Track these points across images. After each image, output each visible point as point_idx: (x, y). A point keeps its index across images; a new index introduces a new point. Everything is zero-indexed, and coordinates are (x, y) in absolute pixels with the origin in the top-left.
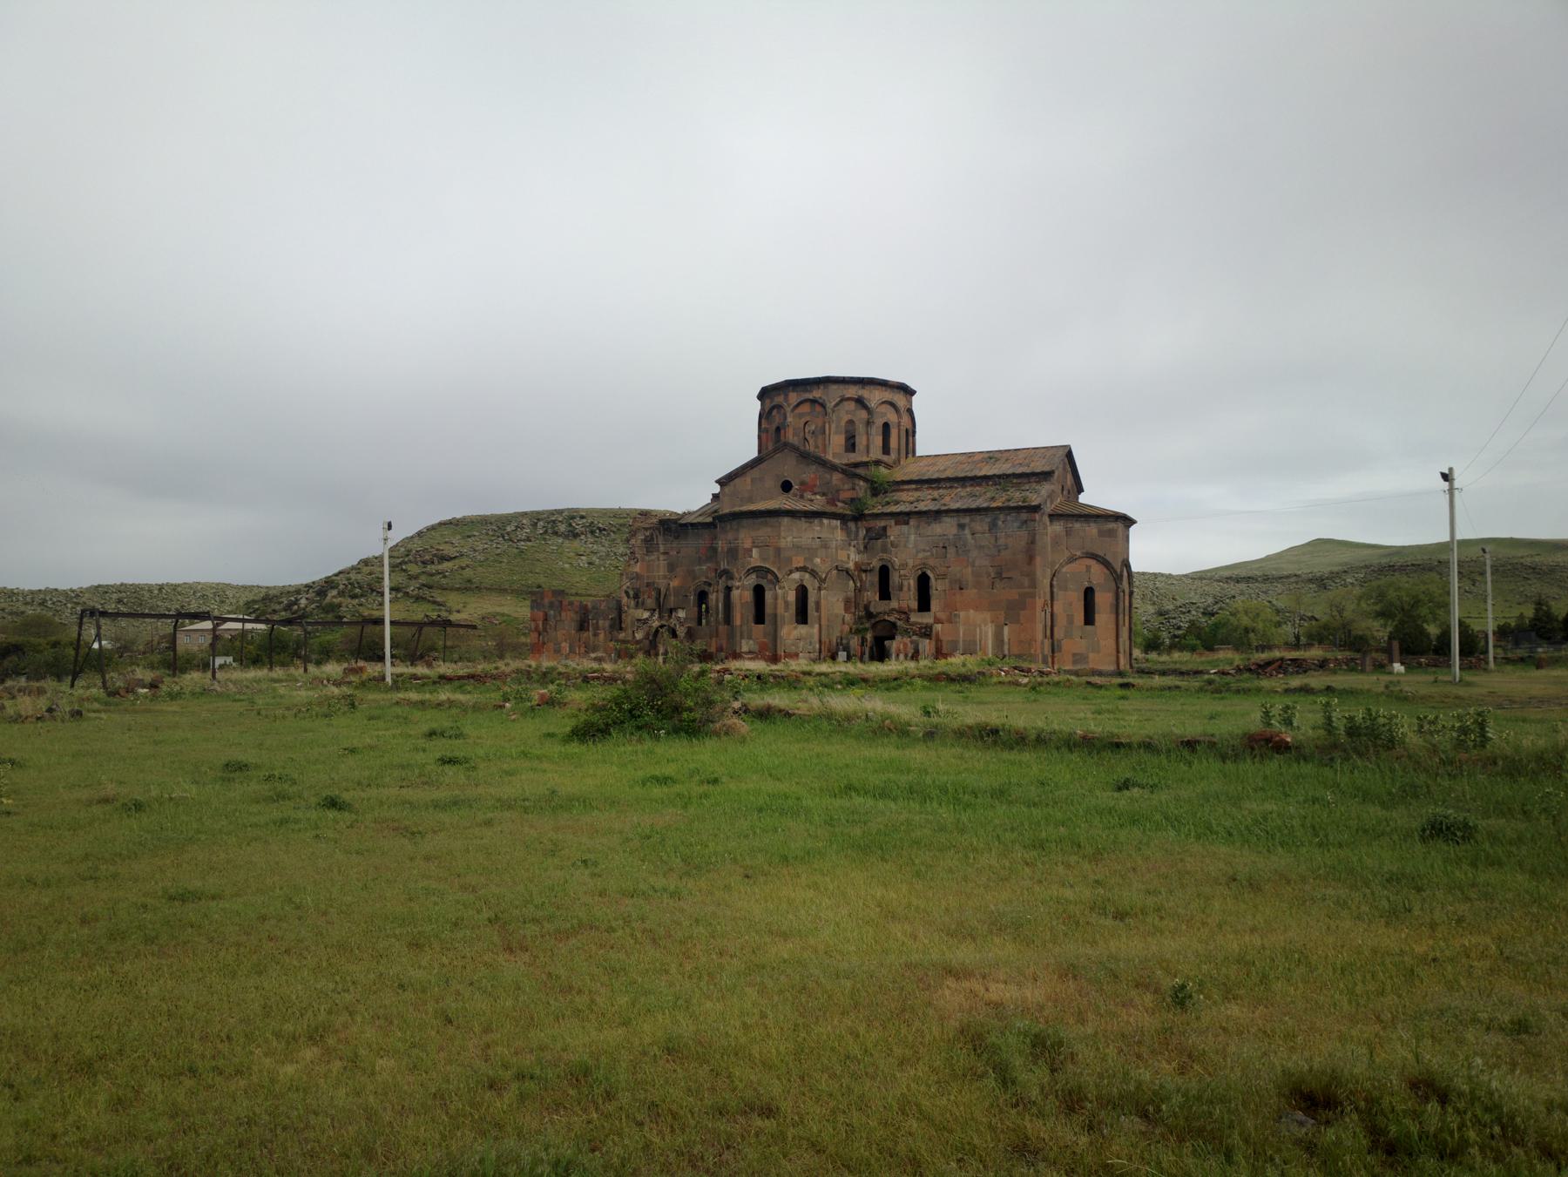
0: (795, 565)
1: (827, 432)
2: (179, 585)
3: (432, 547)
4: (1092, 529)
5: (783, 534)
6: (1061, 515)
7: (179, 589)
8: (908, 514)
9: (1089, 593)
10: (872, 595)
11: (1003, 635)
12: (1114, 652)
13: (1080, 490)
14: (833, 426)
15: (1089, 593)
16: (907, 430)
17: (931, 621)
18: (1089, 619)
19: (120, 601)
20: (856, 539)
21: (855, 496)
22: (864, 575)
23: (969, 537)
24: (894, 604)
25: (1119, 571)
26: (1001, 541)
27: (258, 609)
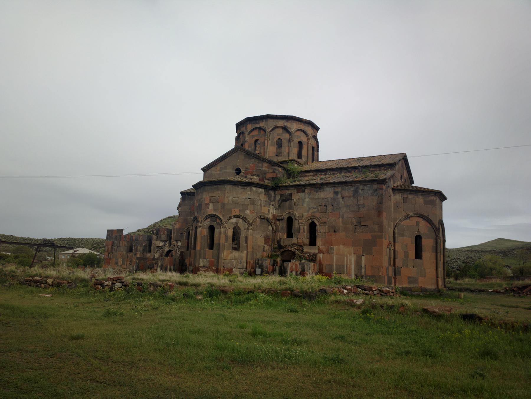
0: (234, 213)
1: (266, 145)
2: (89, 239)
3: (163, 226)
4: (420, 200)
5: (227, 195)
6: (400, 190)
7: (88, 240)
8: (304, 186)
9: (418, 239)
10: (282, 235)
11: (361, 263)
12: (435, 277)
13: (413, 183)
14: (270, 142)
15: (418, 239)
16: (313, 148)
17: (316, 251)
18: (418, 255)
19: (67, 244)
20: (274, 200)
21: (275, 176)
22: (278, 223)
23: (341, 200)
24: (295, 240)
25: (437, 226)
26: (361, 202)
27: (95, 247)
